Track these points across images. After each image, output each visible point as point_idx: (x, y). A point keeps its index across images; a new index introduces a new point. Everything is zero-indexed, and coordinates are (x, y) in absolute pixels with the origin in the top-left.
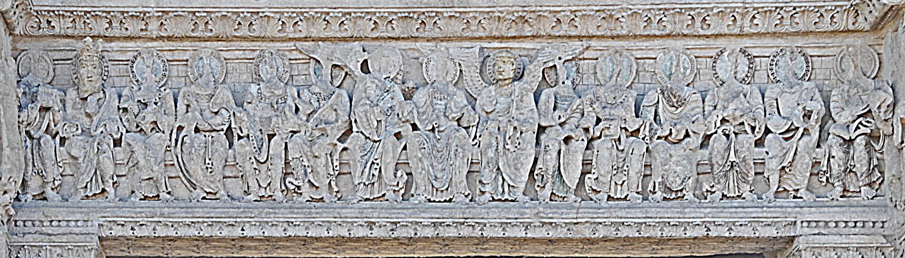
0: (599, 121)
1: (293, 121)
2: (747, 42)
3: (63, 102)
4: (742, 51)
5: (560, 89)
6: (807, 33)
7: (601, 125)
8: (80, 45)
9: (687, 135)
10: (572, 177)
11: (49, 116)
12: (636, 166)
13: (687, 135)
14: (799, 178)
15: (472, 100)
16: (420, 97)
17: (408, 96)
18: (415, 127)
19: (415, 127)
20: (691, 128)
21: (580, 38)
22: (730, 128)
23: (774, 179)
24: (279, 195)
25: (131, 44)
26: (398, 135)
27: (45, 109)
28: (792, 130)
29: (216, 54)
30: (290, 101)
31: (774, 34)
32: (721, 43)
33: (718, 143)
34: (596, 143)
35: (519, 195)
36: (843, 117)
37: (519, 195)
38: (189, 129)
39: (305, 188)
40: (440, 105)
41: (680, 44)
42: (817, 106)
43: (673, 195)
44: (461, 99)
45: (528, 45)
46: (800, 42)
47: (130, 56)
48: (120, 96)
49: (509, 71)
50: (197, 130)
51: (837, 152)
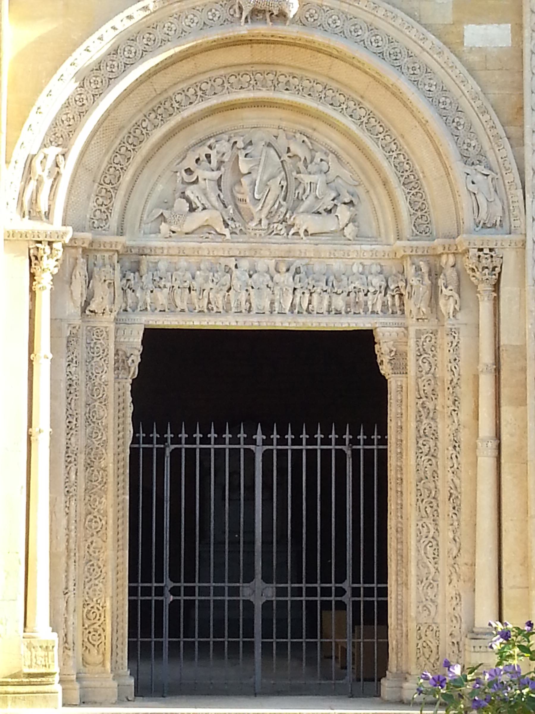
0: (314, 287)
1: (211, 285)
2: (362, 261)
3: (134, 277)
4: (361, 263)
5: (302, 275)
6: (380, 259)
7: (315, 288)
8: (141, 257)
9: (342, 292)
10: (305, 305)
11: (129, 282)
12: (326, 303)
13: (342, 292)
14: (378, 308)
15: (272, 278)
16: (255, 276)
17: (250, 276)
18: (252, 288)
19: (252, 288)
20: (344, 289)
21: (308, 258)
22: (357, 290)
23: (370, 307)
24: (206, 310)
25: (157, 257)
26: (247, 290)
27: (128, 280)
28: (376, 291)
29: (186, 260)
30: (210, 278)
31: (371, 259)
32: (354, 260)
33: (352, 295)
34: (313, 294)
35: (287, 311)
36: (392, 287)
37: (287, 311)
38: (176, 287)
39: (215, 308)
40: (261, 279)
41: (341, 260)
42: (384, 284)
43: (338, 313)
44: (268, 277)
45: (291, 259)
46: (379, 261)
47: (156, 261)
48: (153, 275)
49: (284, 269)
50: (179, 287)
51: (390, 299)
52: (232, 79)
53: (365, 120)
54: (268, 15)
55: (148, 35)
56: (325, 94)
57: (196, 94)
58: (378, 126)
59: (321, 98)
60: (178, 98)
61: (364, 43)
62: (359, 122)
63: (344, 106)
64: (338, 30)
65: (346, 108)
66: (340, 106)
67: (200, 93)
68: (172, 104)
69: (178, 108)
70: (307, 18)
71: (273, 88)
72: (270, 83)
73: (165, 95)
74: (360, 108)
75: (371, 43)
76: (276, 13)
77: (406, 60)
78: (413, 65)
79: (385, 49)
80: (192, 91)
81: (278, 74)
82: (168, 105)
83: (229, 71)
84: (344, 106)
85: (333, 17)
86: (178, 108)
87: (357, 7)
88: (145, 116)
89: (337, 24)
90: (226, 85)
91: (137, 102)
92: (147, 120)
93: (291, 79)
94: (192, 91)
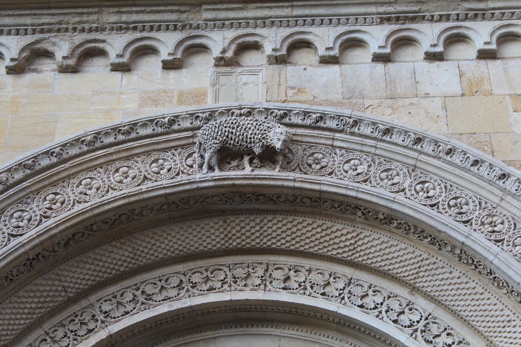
52: (196, 278)
53: (421, 326)
54: (246, 159)
55: (52, 196)
56: (350, 292)
57: (134, 300)
58: (444, 335)
59: (343, 298)
60: (106, 307)
61: (405, 194)
62: (410, 330)
63: (384, 308)
64: (361, 178)
65: (387, 311)
66: (375, 308)
67: (142, 299)
68: (94, 316)
69: (103, 322)
70: (310, 166)
71: (262, 287)
72: (258, 281)
73: (84, 303)
74: (410, 310)
75: (417, 193)
76: (257, 150)
77: (477, 213)
78: (490, 219)
79: (440, 199)
80: (129, 296)
81: (271, 268)
82: (87, 317)
83: (191, 265)
84: (384, 308)
85: (352, 162)
86: (103, 322)
87: (389, 142)
88: (47, 334)
89: (359, 171)
90: (187, 286)
91: (34, 305)
92: (49, 340)
93: (292, 273)
94: (129, 296)
